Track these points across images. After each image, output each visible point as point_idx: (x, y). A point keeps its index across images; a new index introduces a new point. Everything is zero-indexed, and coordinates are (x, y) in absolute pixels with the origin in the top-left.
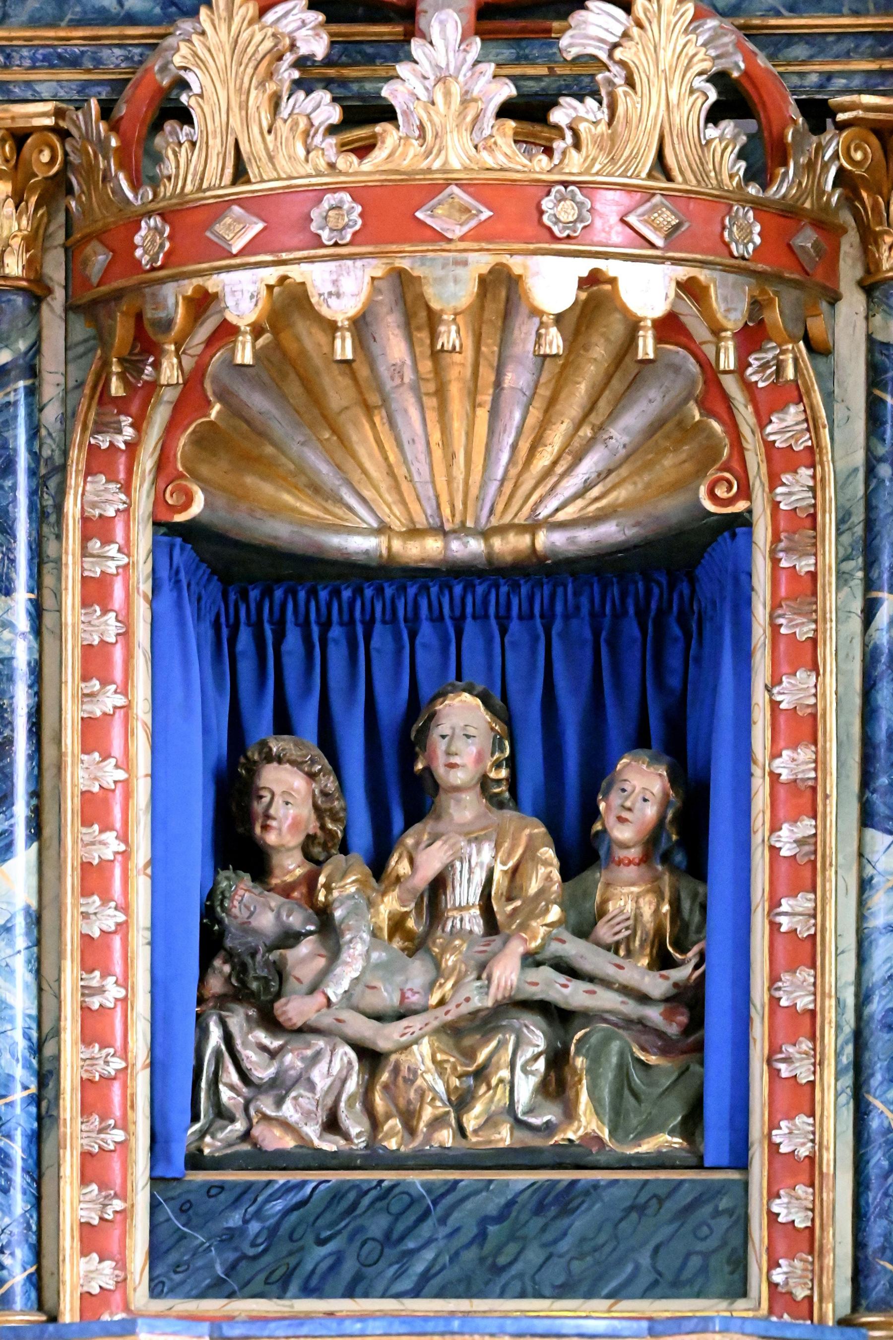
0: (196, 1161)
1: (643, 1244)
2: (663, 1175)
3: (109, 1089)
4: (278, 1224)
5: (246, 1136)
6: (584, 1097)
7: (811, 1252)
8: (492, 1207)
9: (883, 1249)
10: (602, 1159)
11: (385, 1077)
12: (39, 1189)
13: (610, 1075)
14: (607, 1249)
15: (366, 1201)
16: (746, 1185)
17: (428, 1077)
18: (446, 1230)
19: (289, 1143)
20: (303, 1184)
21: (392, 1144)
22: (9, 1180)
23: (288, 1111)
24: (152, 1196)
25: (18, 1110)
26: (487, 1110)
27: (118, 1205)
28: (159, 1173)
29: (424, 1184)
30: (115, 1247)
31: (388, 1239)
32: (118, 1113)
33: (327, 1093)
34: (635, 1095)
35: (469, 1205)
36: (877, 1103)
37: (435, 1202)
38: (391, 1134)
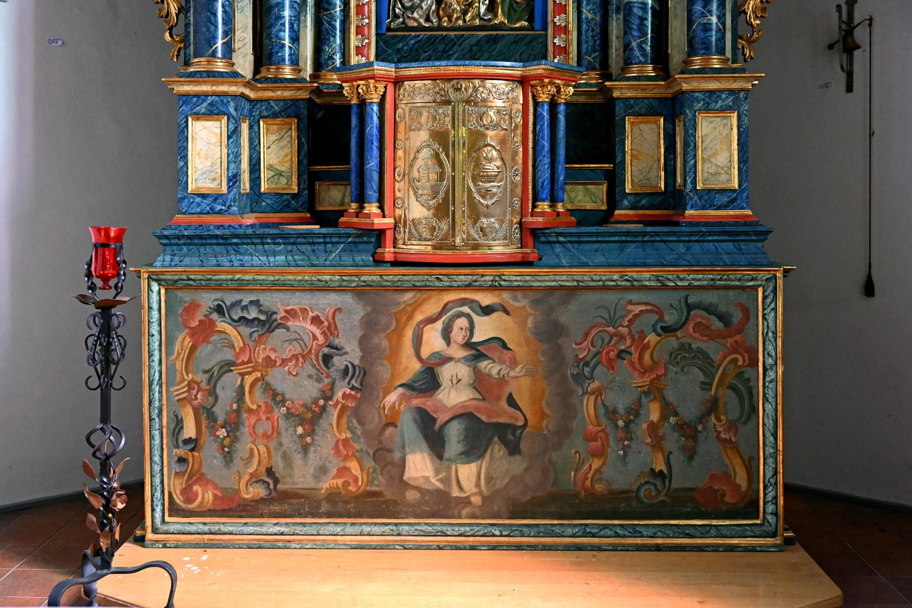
0: (389, 29)
1: (517, 52)
2: (523, 32)
3: (364, 7)
4: (413, 47)
5: (403, 22)
6: (500, 11)
7: (565, 54)
8: (473, 42)
9: (586, 53)
10: (505, 28)
11: (443, 6)
12: (344, 36)
13: (507, 4)
14: (507, 54)
15: (438, 40)
16: (546, 35)
17: (455, 6)
18: (461, 48)
19: (416, 24)
20: (420, 35)
21: (445, 24)
22: (335, 34)
23: (415, 15)
24: (376, 39)
25: (338, 13)
26: (472, 15)
27: (366, 41)
28: (378, 32)
29: (455, 35)
30: (366, 53)
31: (445, 51)
32: (367, 15)
33: (426, 10)
34: (514, 10)
35: (467, 41)
36: (584, 10)
37: (458, 41)
38: (445, 21)
